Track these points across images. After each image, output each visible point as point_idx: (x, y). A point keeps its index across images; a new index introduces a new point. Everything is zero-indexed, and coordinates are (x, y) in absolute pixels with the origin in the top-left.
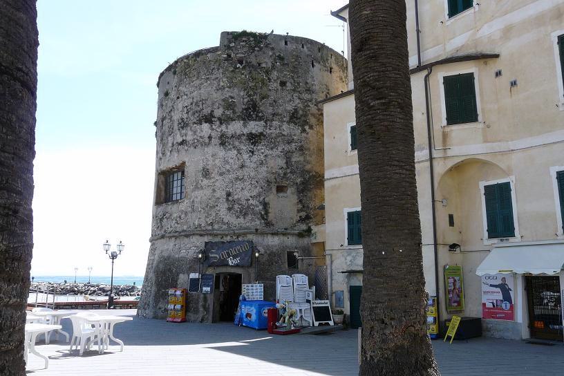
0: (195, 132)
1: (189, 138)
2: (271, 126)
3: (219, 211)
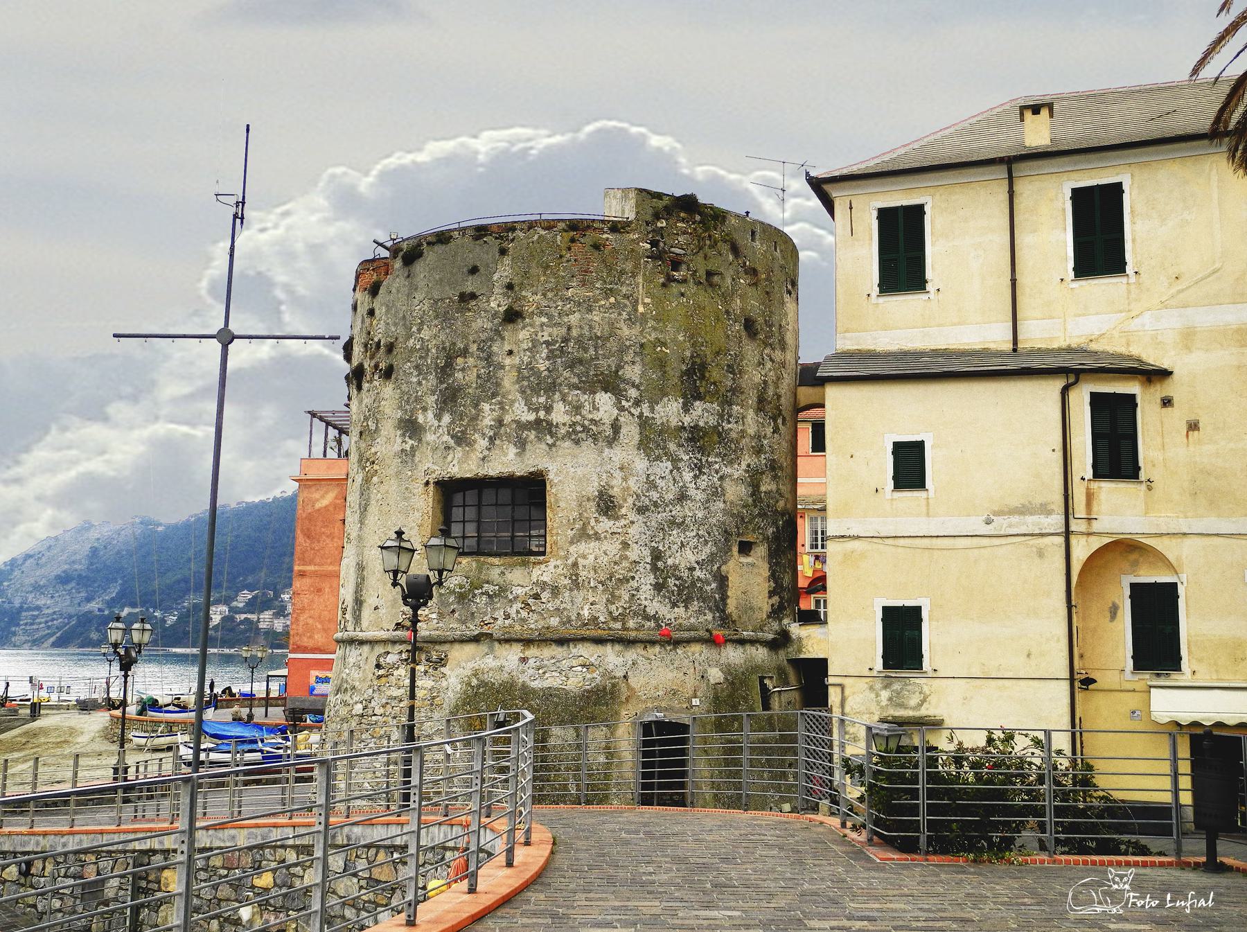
0: (577, 409)
1: (560, 415)
2: (730, 416)
3: (637, 590)
